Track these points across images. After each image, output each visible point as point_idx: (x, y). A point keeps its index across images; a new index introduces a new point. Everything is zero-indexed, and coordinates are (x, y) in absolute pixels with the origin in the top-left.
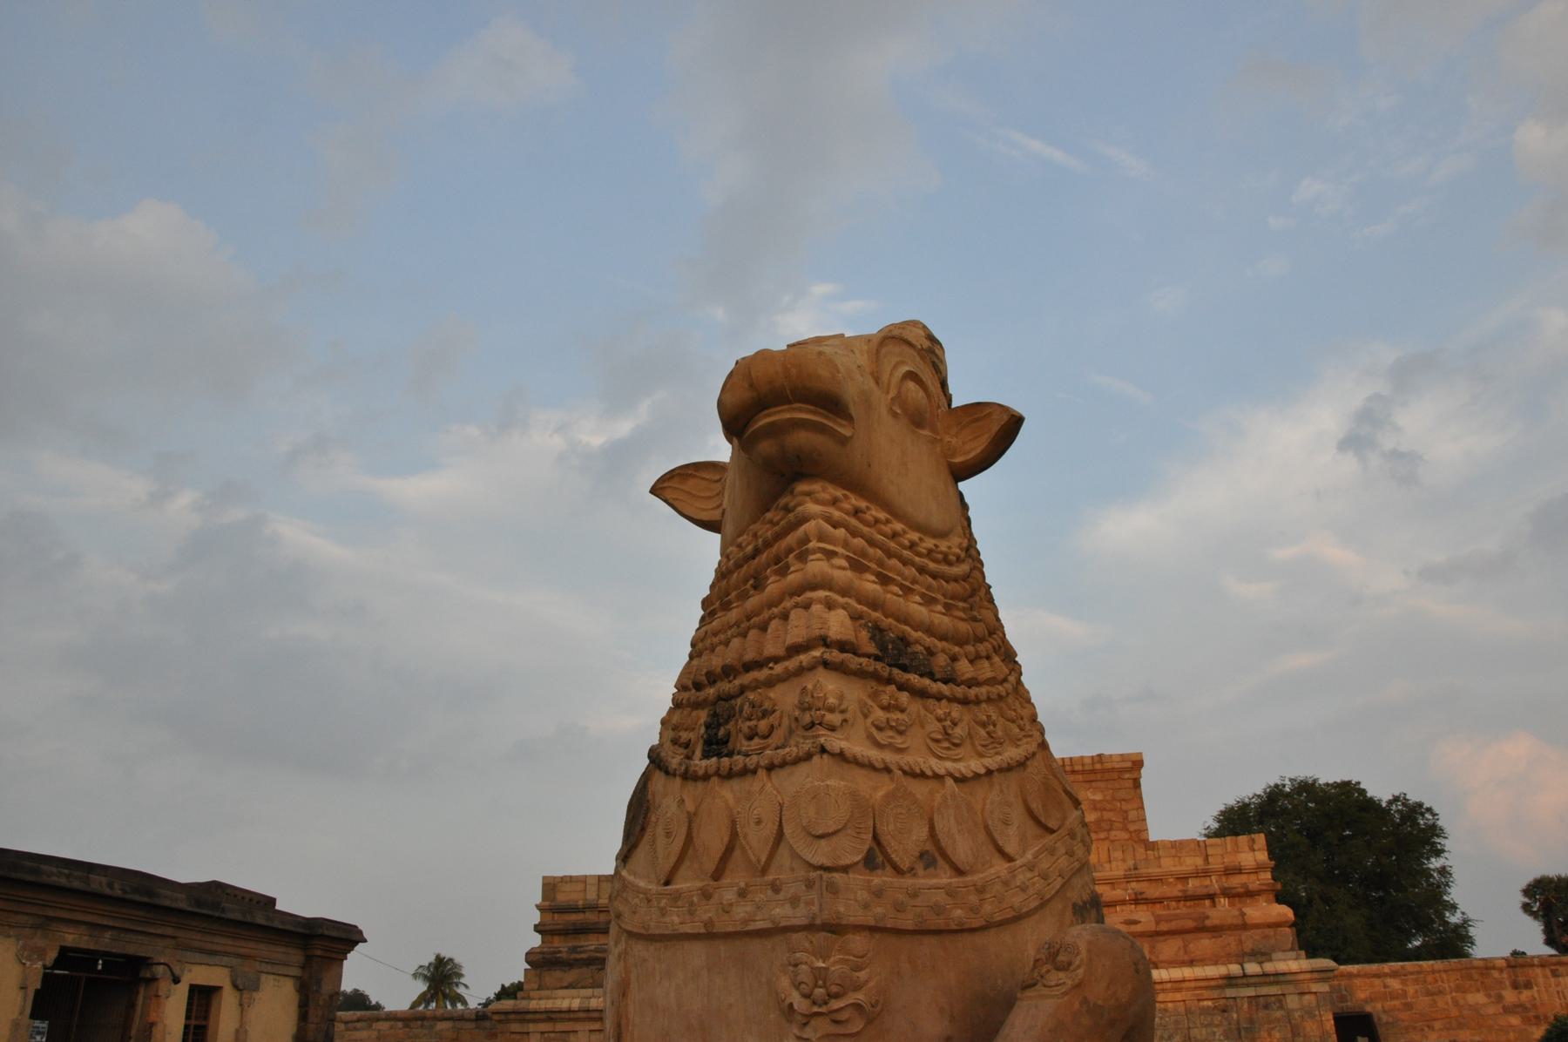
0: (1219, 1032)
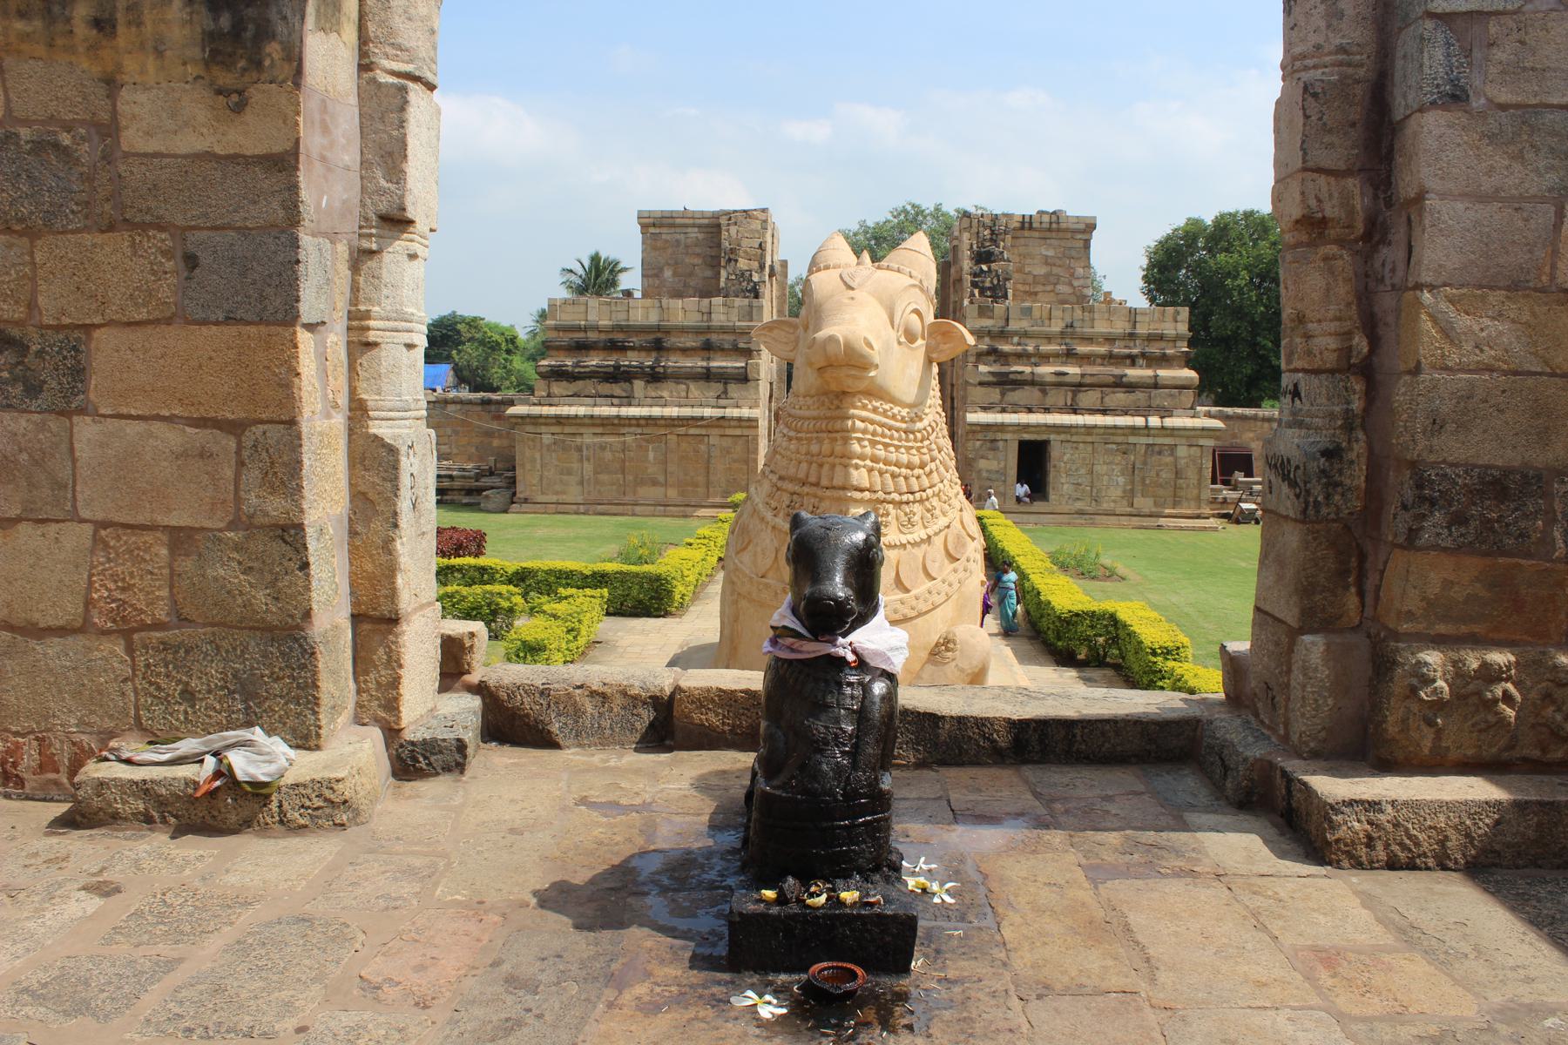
0: (1117, 469)
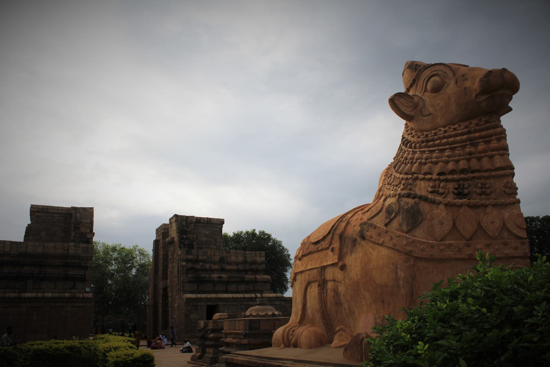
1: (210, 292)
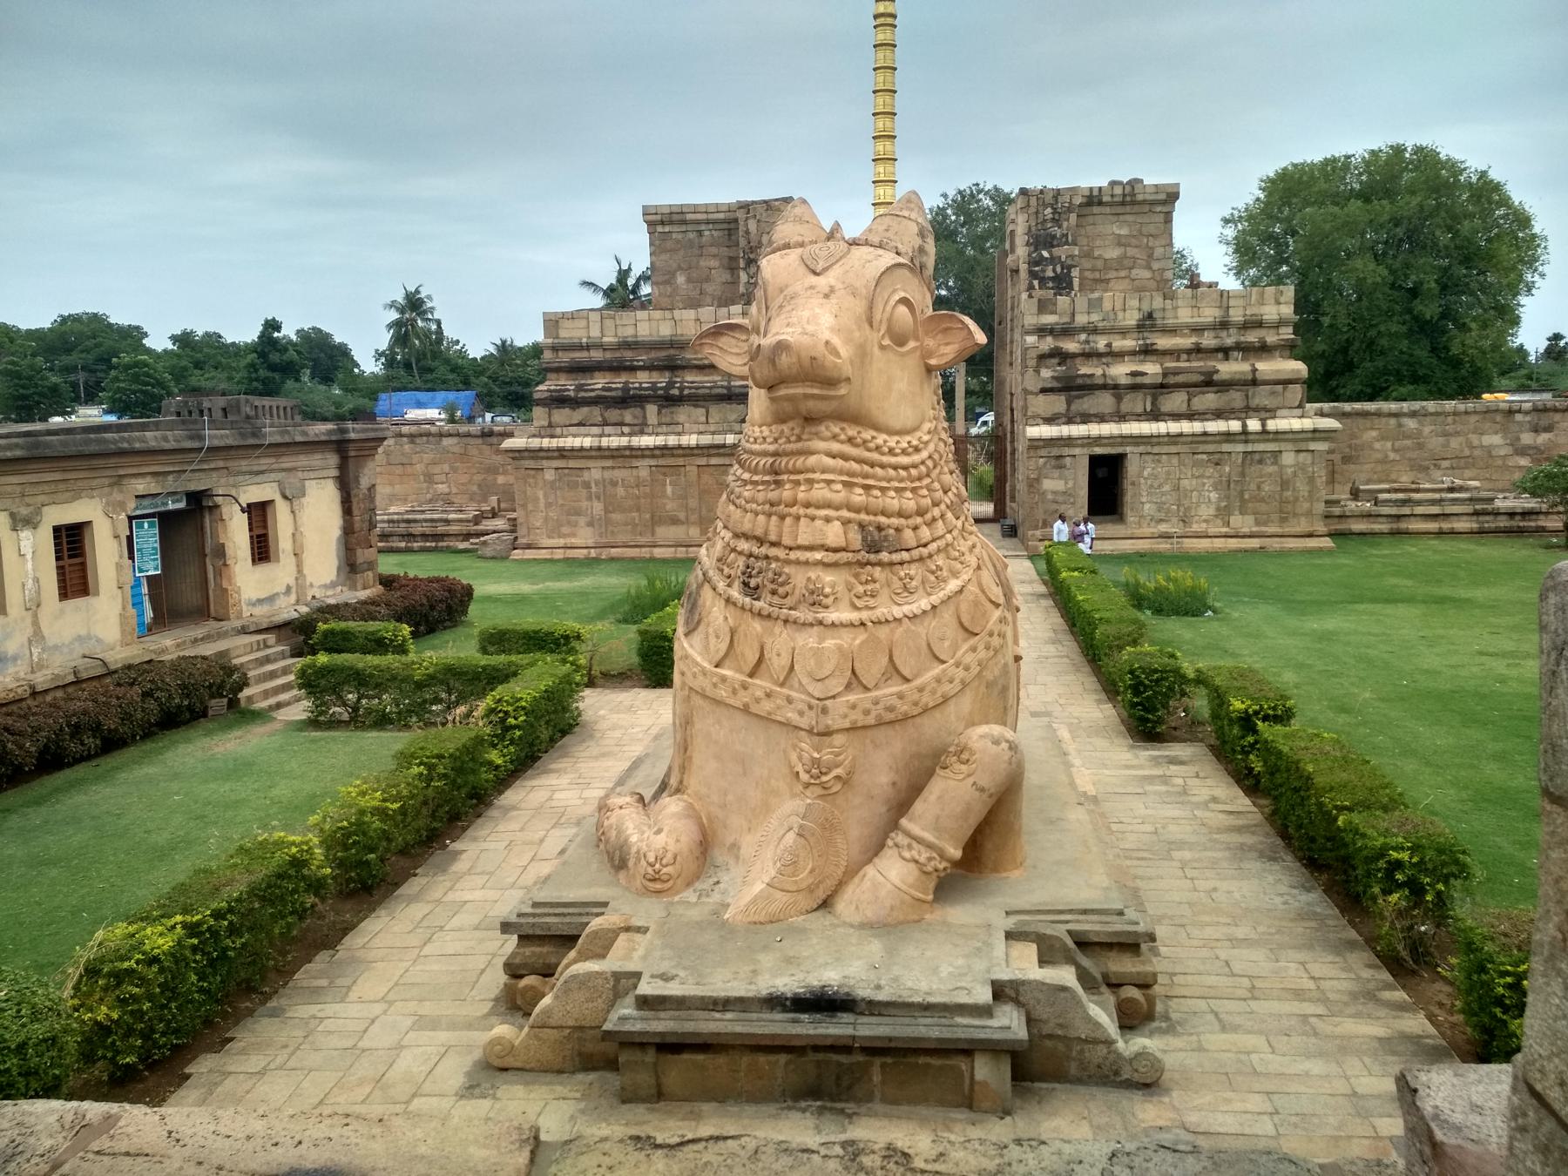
0: (1208, 483)
1: (1102, 419)
